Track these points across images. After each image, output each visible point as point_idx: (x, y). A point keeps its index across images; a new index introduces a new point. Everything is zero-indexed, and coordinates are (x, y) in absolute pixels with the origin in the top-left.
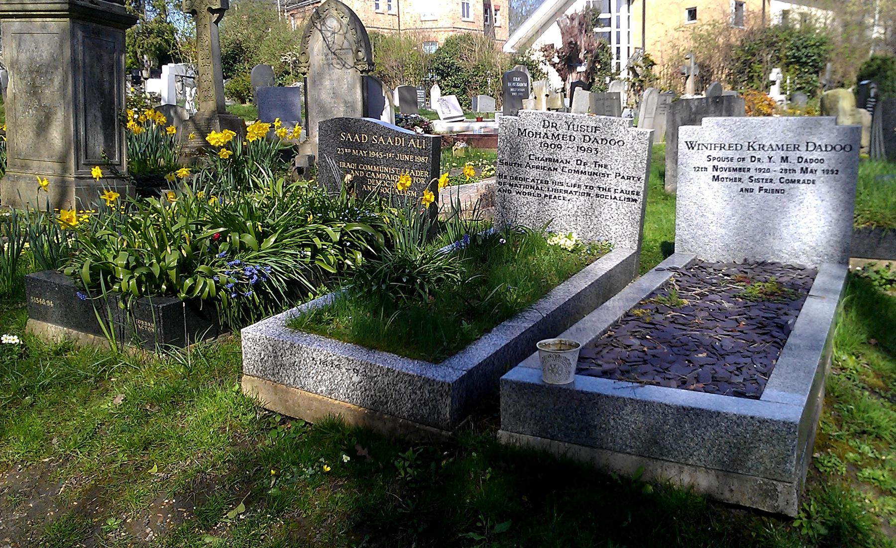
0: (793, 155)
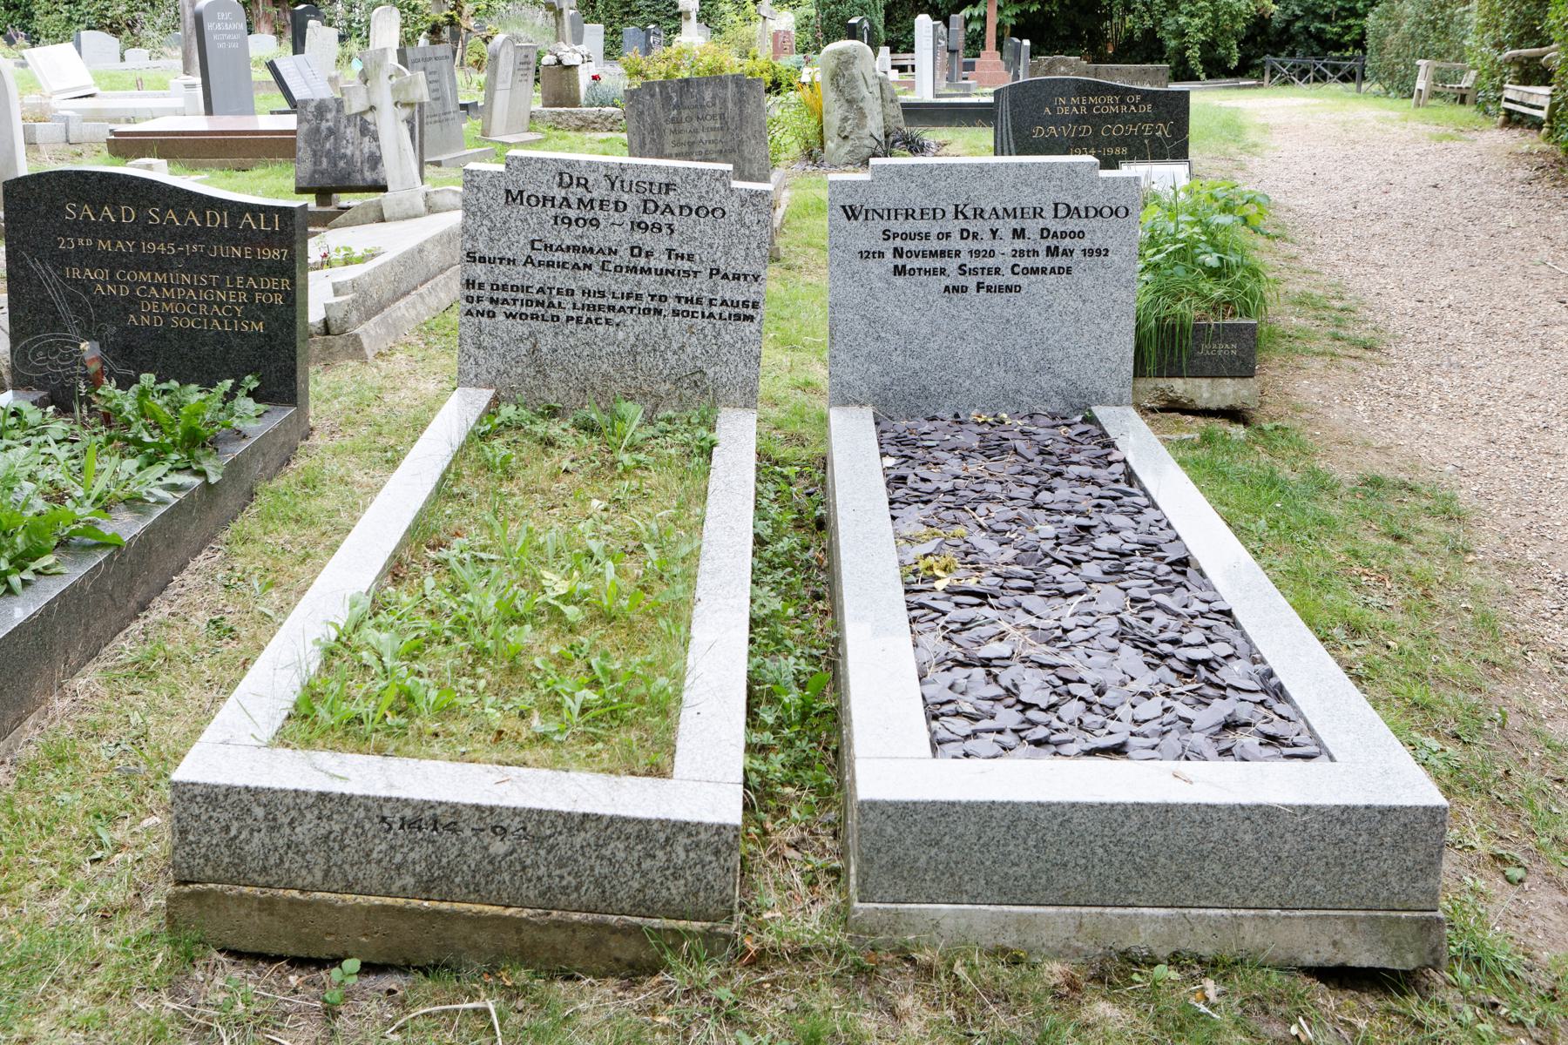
0: (1032, 226)
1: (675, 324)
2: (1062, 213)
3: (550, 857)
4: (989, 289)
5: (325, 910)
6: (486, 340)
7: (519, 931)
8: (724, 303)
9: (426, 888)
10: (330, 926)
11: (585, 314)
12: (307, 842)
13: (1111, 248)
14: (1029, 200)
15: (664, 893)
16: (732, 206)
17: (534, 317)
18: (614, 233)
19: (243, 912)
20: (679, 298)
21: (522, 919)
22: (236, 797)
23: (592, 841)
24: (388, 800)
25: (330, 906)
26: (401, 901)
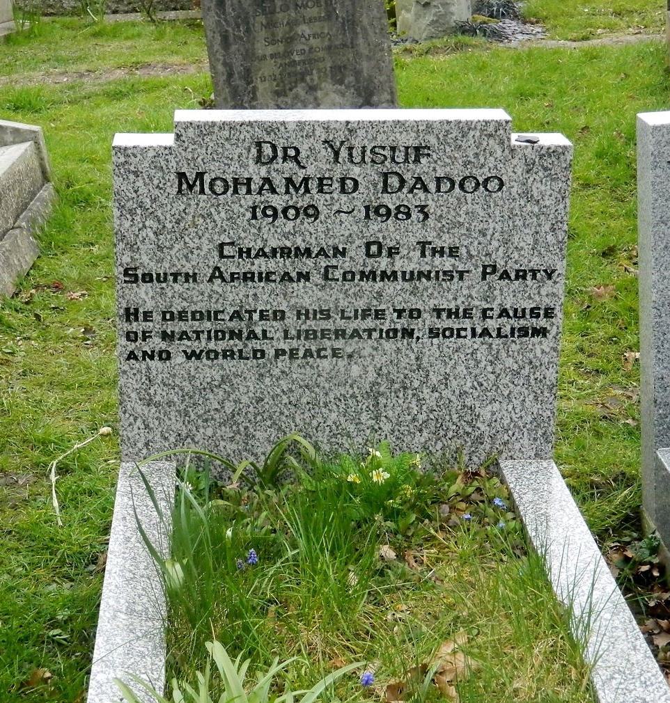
1: (431, 348)
8: (504, 313)
16: (513, 172)
18: (340, 224)
20: (438, 312)
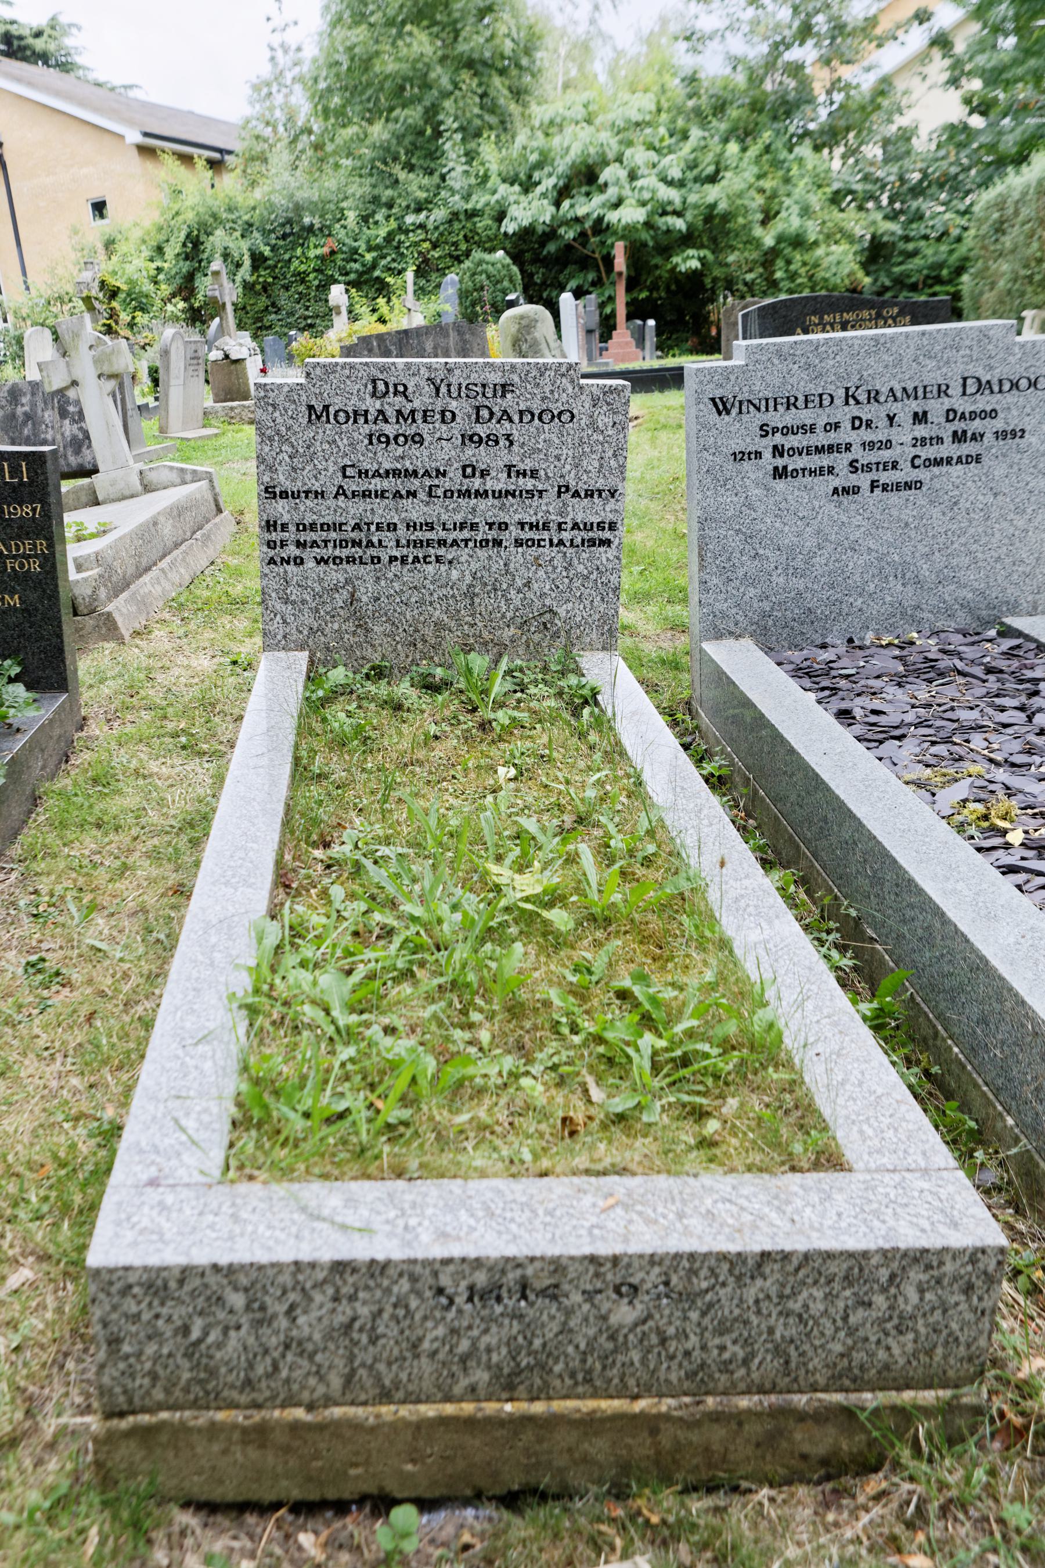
0: (936, 408)
1: (518, 556)
2: (971, 389)
3: (706, 1321)
4: (885, 488)
5: (348, 1433)
6: (294, 593)
7: (654, 1431)
8: (575, 526)
9: (508, 1385)
10: (357, 1453)
11: (411, 552)
12: (317, 1337)
13: (1028, 428)
14: (933, 377)
15: (882, 1354)
16: (582, 407)
17: (351, 560)
18: (441, 450)
19: (216, 1448)
20: (522, 525)
21: (660, 1416)
22: (197, 1282)
23: (773, 1292)
24: (447, 1262)
25: (356, 1426)
26: (468, 1408)
